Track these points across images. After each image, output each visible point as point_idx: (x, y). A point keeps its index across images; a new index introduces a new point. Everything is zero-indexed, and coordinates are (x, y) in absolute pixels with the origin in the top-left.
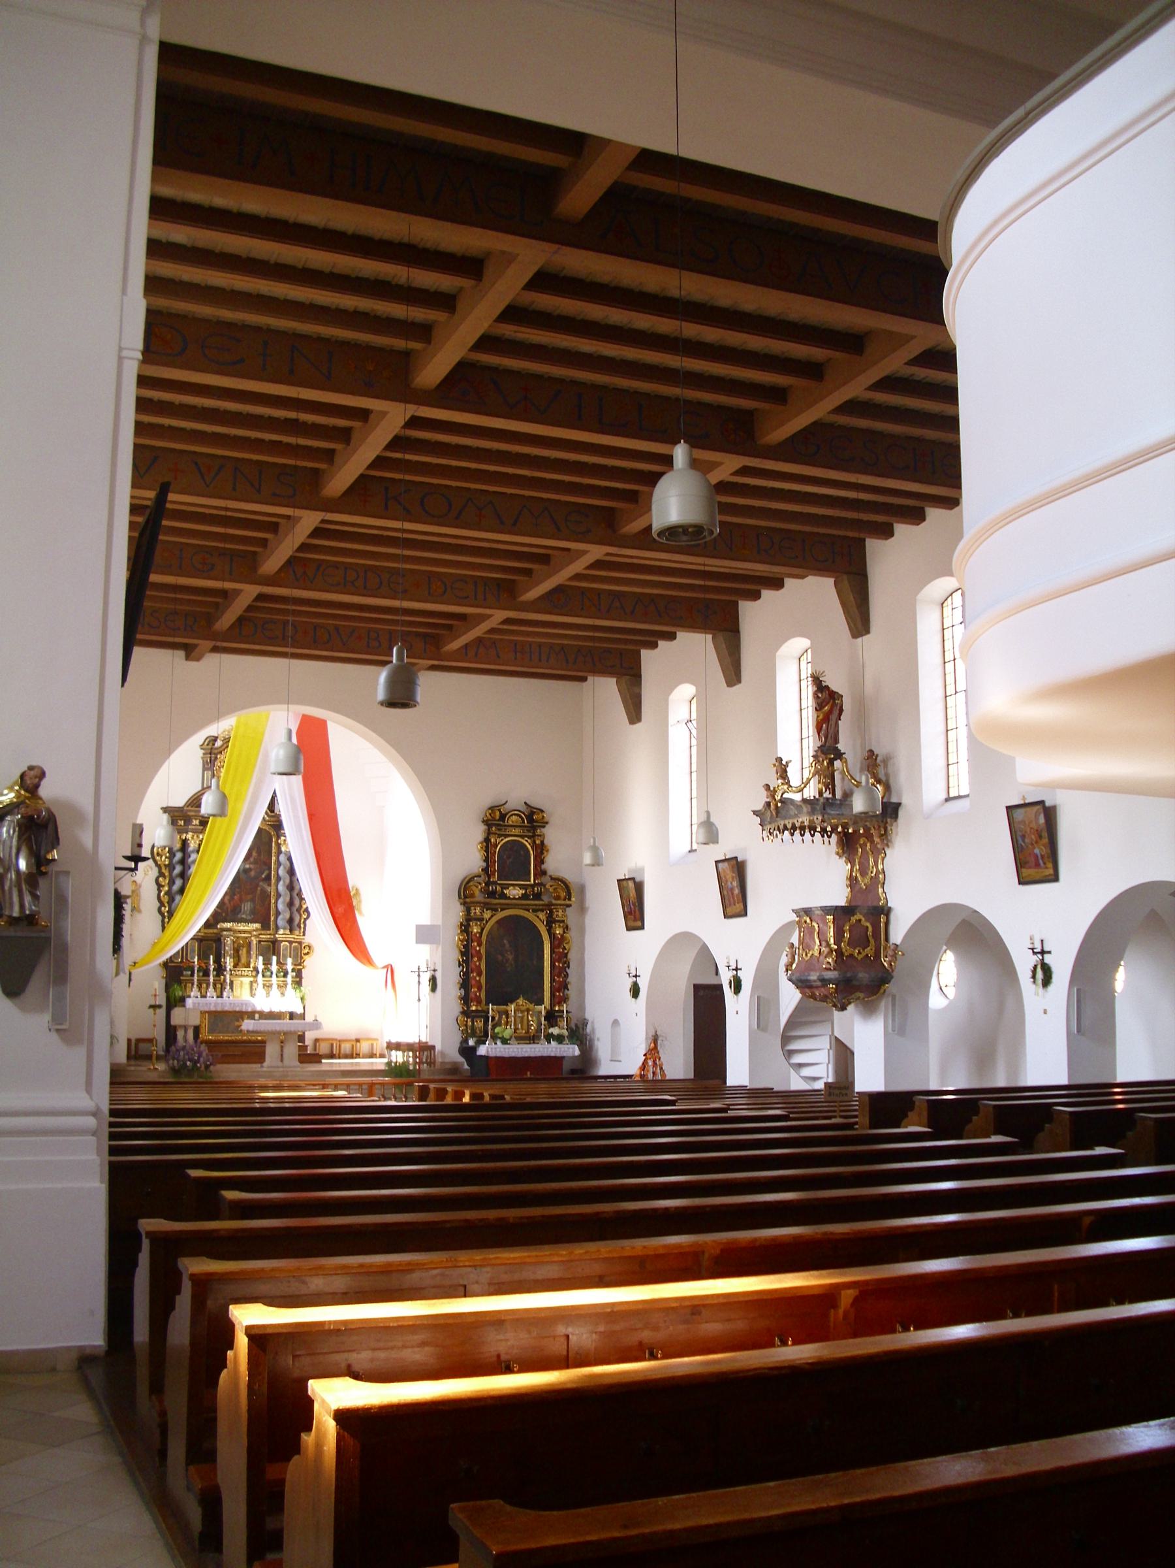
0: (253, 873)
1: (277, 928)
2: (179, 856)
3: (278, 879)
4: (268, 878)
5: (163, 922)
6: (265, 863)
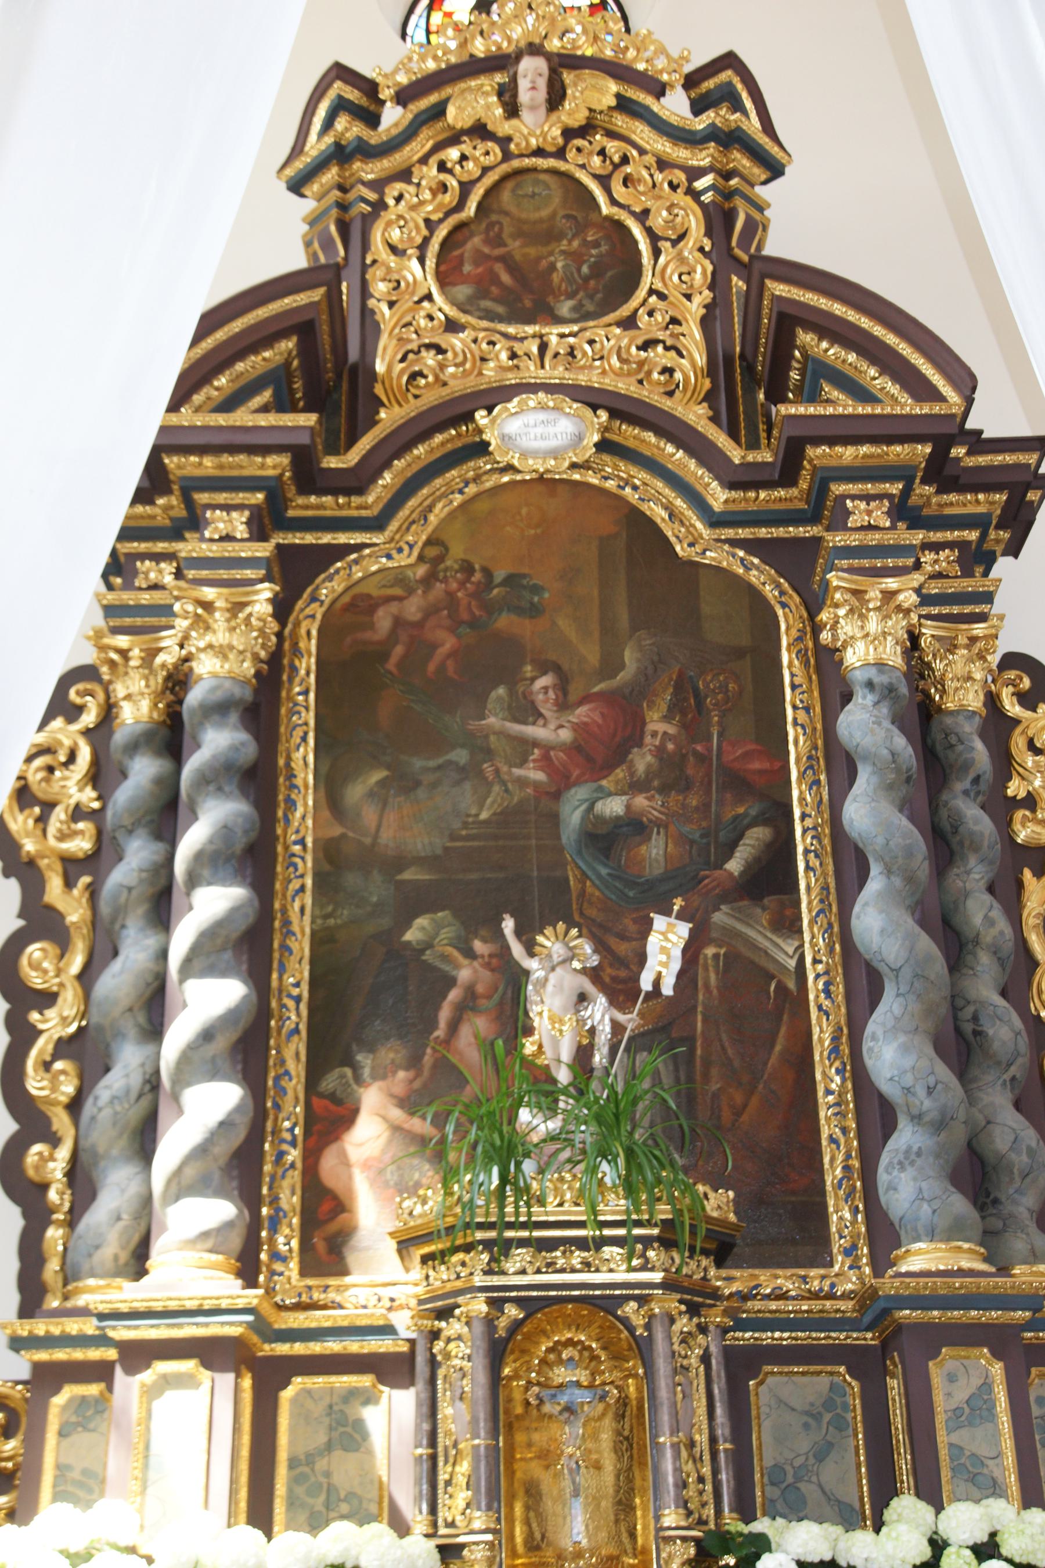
0: (655, 852)
1: (883, 1236)
2: (143, 771)
3: (850, 863)
4: (773, 877)
5: (31, 1251)
6: (737, 783)
